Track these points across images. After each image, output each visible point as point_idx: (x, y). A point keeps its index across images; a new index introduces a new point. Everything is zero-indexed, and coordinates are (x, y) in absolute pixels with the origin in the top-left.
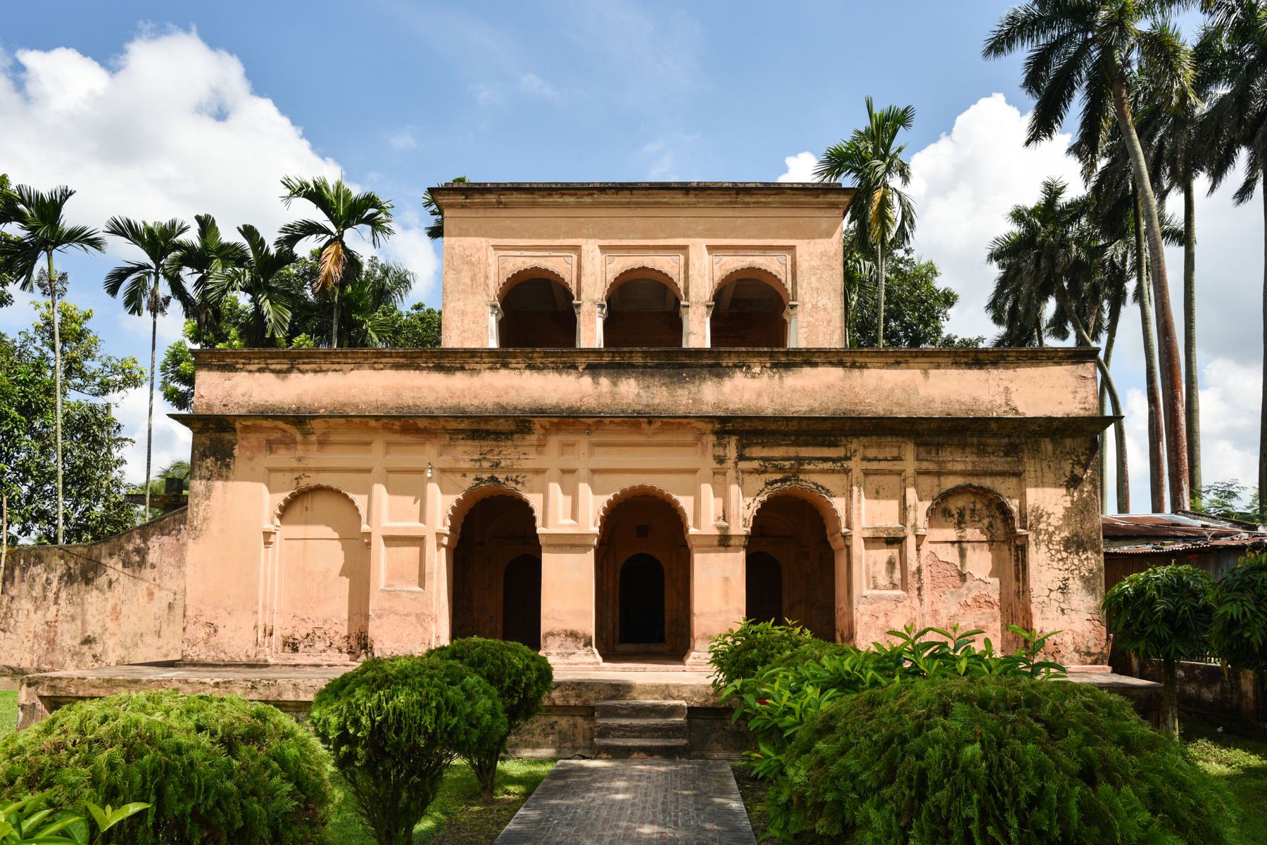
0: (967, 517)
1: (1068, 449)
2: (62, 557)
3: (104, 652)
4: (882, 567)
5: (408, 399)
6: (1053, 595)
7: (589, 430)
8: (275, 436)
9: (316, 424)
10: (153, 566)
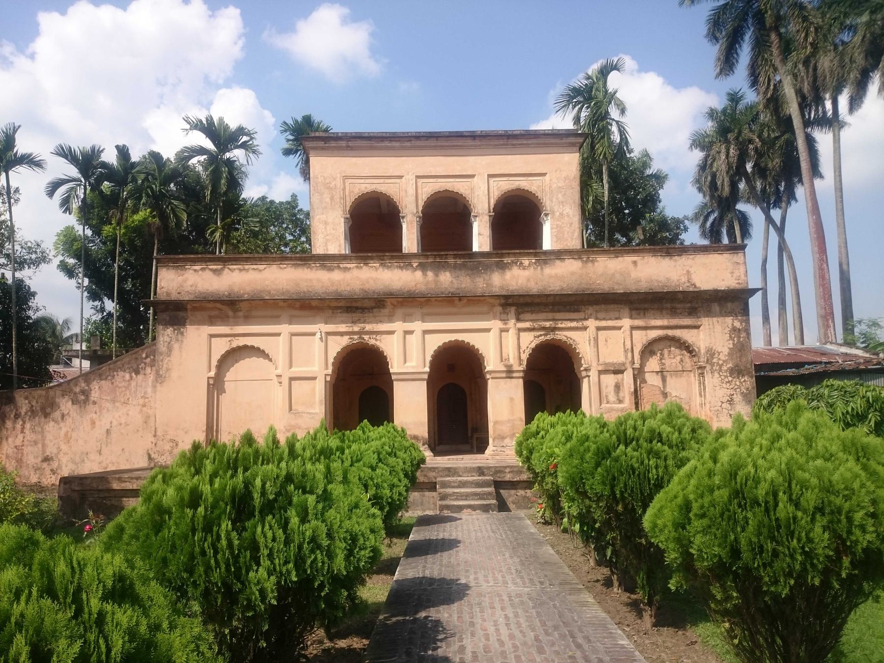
3: (60, 467)
4: (611, 389)
5: (304, 287)
6: (724, 405)
7: (421, 305)
8: (214, 313)
9: (242, 305)
10: (95, 403)
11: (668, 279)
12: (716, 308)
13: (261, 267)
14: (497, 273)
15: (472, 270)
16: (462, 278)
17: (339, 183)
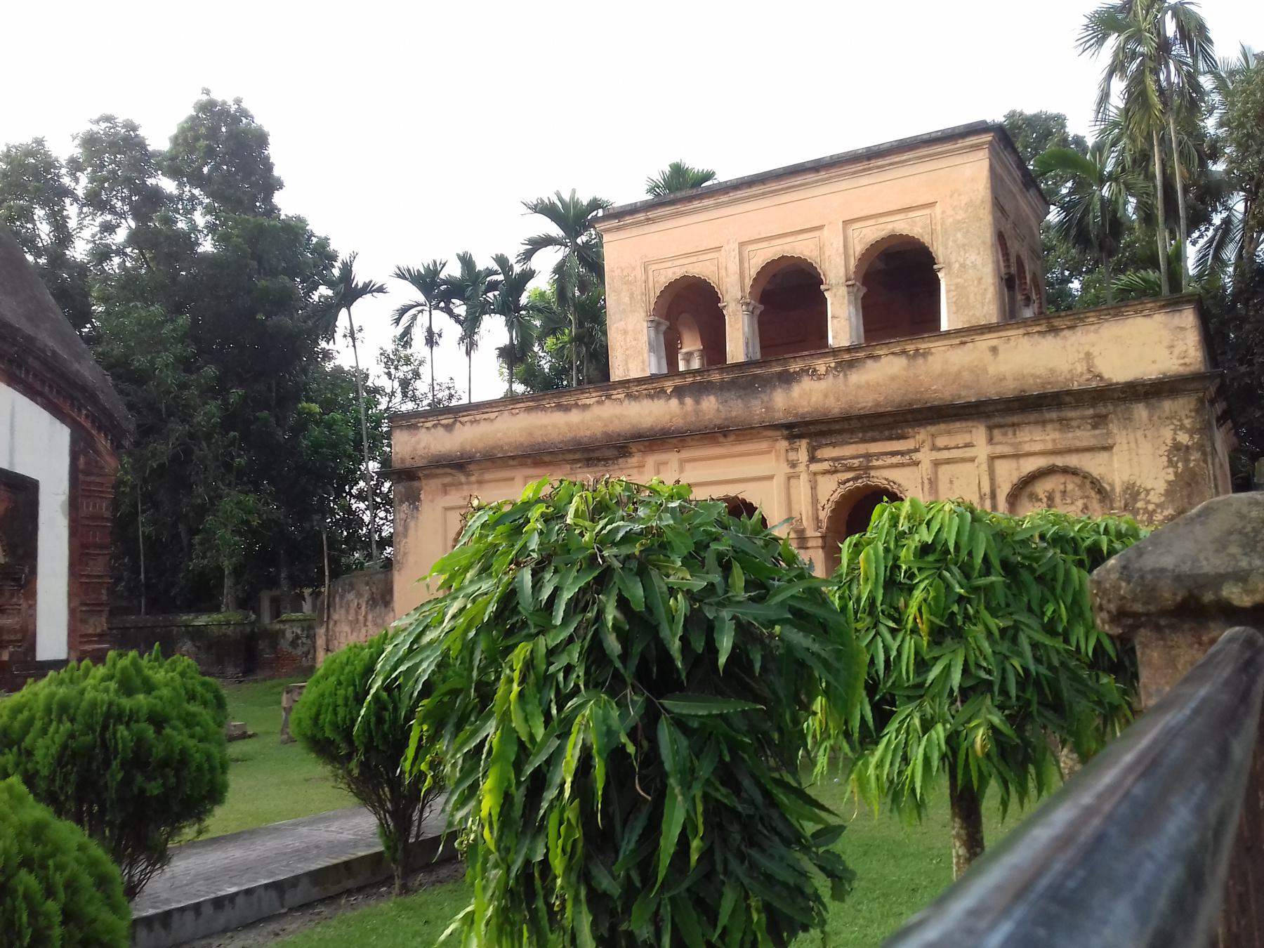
0: (1058, 500)
1: (1167, 413)
2: (367, 584)
5: (539, 437)
11: (1052, 371)
12: (1141, 411)
13: (493, 416)
14: (779, 390)
15: (744, 389)
16: (731, 403)
17: (639, 274)
